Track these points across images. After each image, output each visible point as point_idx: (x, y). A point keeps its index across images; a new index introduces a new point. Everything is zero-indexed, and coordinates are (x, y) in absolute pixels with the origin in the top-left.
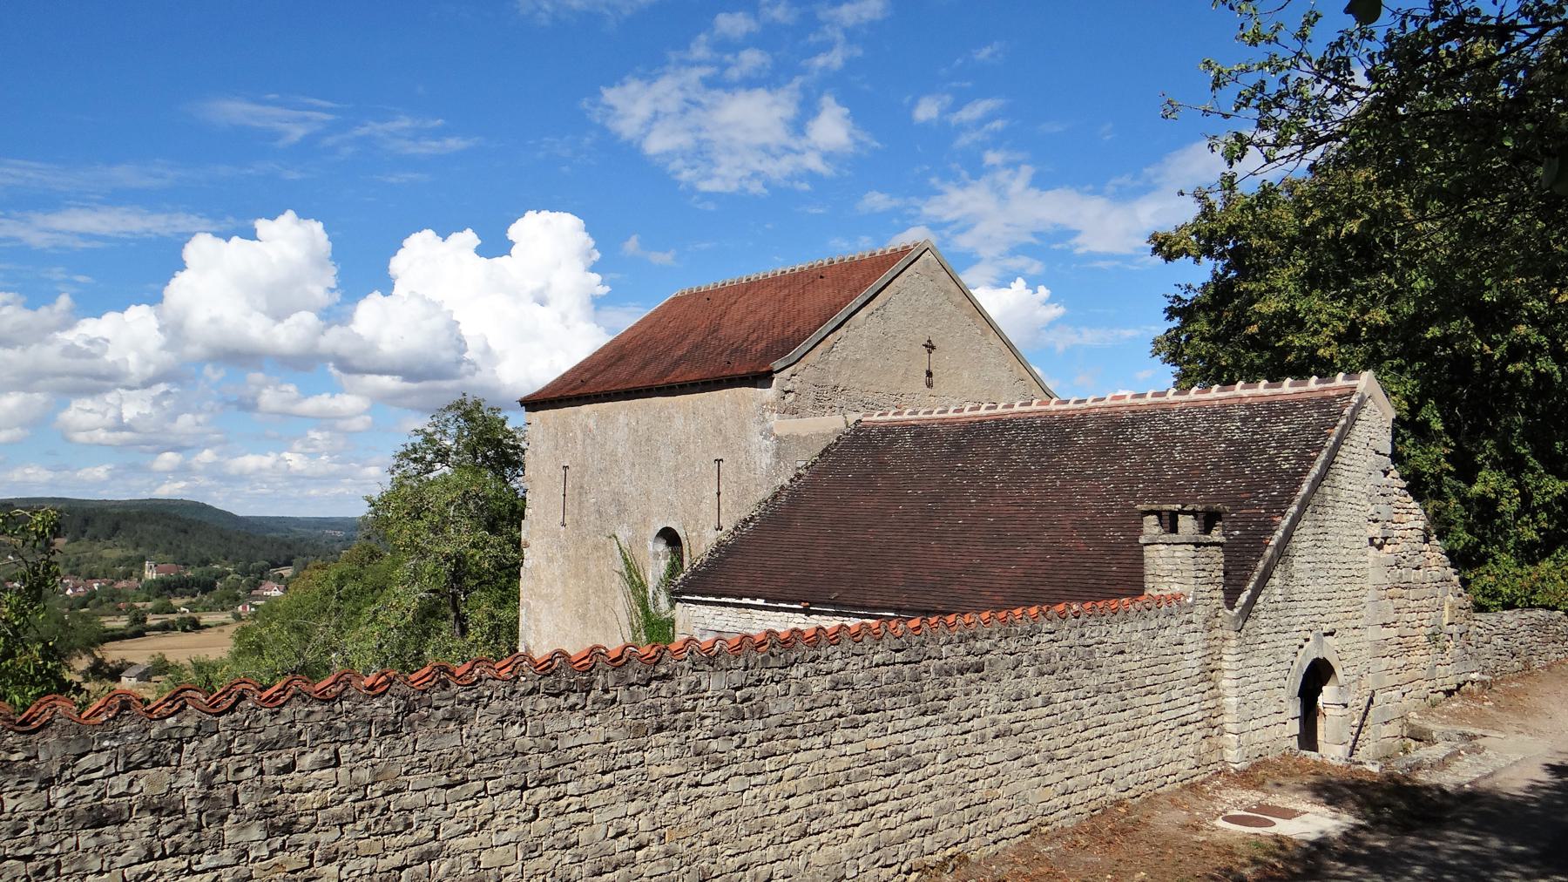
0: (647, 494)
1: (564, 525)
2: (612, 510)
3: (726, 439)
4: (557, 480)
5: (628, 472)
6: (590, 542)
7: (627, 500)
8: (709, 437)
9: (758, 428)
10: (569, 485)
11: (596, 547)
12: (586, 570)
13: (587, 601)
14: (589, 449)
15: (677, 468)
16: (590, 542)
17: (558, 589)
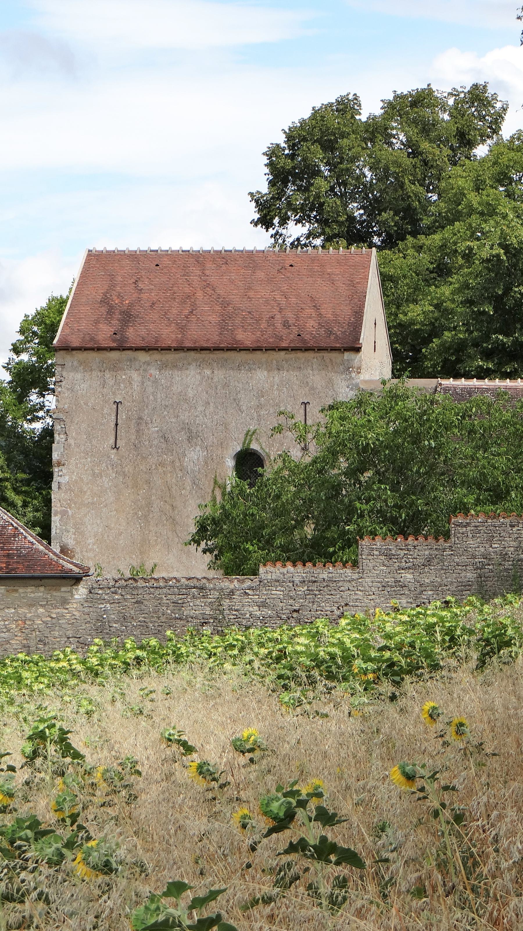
0: (226, 425)
1: (116, 447)
2: (182, 436)
3: (313, 388)
4: (105, 411)
5: (200, 409)
6: (152, 460)
7: (200, 429)
8: (295, 387)
9: (344, 384)
10: (123, 416)
11: (162, 464)
12: (148, 482)
13: (149, 504)
14: (150, 390)
15: (260, 406)
16: (152, 460)
17: (110, 497)
